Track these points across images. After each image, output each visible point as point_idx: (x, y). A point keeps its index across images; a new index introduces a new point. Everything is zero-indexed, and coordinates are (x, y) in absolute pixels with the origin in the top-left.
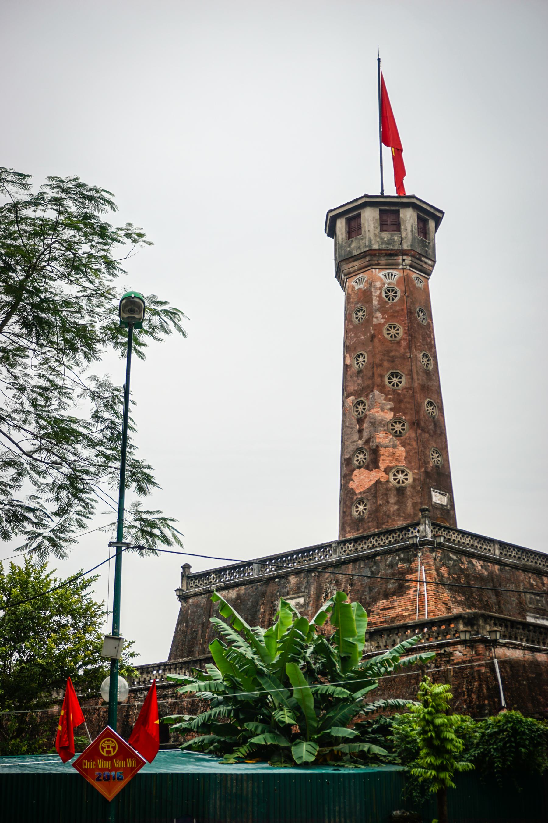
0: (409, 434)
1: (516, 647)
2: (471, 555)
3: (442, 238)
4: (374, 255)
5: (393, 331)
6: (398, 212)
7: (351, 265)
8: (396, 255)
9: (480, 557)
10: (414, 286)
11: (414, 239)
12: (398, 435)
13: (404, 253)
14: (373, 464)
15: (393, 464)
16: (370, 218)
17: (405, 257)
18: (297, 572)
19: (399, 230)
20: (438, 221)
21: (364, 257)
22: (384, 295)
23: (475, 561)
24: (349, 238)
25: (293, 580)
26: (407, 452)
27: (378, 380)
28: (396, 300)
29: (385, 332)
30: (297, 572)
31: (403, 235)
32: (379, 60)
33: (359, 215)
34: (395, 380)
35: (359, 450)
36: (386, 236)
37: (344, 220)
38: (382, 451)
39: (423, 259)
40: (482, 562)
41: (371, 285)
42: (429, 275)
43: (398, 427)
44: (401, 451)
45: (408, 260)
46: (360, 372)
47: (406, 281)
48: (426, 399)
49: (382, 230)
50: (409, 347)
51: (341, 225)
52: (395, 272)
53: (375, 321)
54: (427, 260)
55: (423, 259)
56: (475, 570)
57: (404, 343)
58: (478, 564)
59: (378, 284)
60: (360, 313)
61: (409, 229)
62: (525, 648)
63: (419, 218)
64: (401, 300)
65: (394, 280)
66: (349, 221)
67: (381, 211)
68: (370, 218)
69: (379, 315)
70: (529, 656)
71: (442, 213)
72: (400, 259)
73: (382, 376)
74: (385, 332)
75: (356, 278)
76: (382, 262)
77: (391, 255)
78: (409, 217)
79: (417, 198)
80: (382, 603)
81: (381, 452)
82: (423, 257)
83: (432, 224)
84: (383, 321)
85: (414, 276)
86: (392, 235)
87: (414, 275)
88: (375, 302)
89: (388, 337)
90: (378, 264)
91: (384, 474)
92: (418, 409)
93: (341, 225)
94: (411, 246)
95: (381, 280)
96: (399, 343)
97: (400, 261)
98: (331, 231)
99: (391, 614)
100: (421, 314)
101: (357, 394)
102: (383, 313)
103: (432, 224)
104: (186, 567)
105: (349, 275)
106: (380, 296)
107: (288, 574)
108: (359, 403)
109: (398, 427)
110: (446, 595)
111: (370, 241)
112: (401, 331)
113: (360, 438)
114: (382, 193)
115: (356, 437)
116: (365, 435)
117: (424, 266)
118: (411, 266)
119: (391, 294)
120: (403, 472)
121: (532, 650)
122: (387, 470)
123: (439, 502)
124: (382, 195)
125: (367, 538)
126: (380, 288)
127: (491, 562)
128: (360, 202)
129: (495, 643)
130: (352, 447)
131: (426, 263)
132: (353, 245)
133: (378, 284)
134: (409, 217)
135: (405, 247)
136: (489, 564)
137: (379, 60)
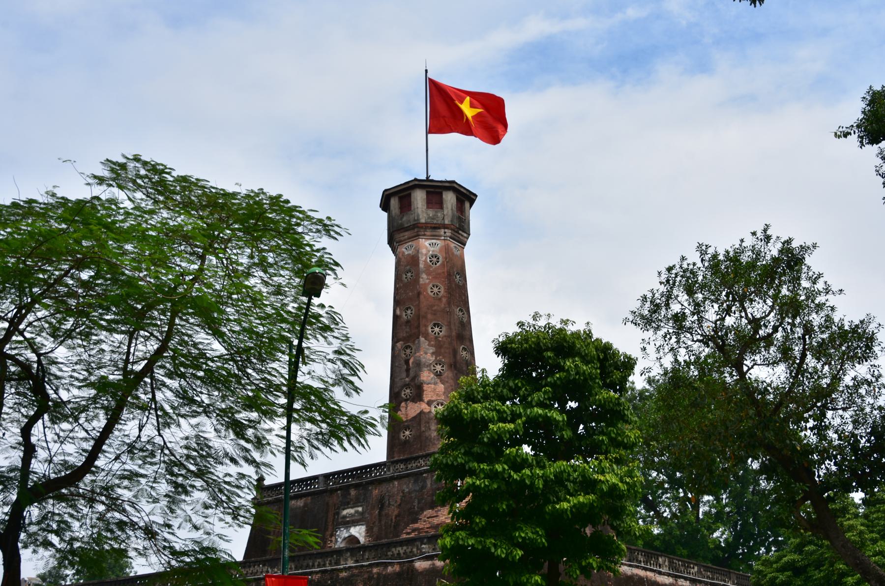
0: (448, 374)
3: (476, 215)
4: (422, 228)
5: (436, 290)
6: (441, 194)
7: (402, 235)
8: (439, 228)
10: (453, 254)
11: (453, 216)
12: (439, 375)
13: (445, 227)
14: (418, 397)
15: (434, 398)
16: (419, 198)
18: (356, 486)
19: (442, 208)
20: (472, 202)
21: (413, 229)
22: (428, 260)
24: (401, 212)
25: (353, 492)
26: (445, 388)
27: (423, 329)
28: (438, 264)
29: (429, 290)
30: (356, 486)
31: (445, 213)
32: (426, 71)
33: (410, 195)
34: (437, 329)
35: (407, 386)
36: (431, 213)
37: (396, 200)
38: (425, 387)
41: (418, 251)
42: (465, 245)
43: (439, 368)
44: (441, 387)
45: (449, 233)
46: (408, 322)
47: (447, 249)
49: (428, 207)
50: (449, 303)
51: (394, 203)
52: (438, 242)
57: (444, 300)
59: (424, 251)
60: (409, 274)
61: (450, 207)
63: (457, 199)
64: (443, 265)
65: (437, 248)
66: (401, 199)
68: (419, 198)
69: (424, 276)
71: (476, 196)
73: (426, 326)
74: (429, 290)
75: (406, 245)
76: (428, 233)
78: (450, 198)
80: (428, 512)
81: (425, 388)
82: (460, 230)
83: (467, 204)
85: (452, 245)
86: (436, 212)
87: (453, 244)
88: (422, 266)
90: (424, 235)
91: (427, 406)
92: (455, 352)
93: (394, 203)
95: (427, 248)
96: (440, 299)
97: (442, 233)
98: (385, 205)
99: (436, 521)
101: (406, 339)
102: (428, 274)
103: (467, 204)
105: (401, 243)
106: (425, 261)
107: (349, 487)
108: (407, 347)
109: (439, 368)
111: (418, 216)
112: (442, 290)
113: (407, 376)
114: (427, 178)
115: (404, 375)
116: (412, 373)
119: (435, 259)
122: (429, 403)
124: (428, 179)
125: (416, 459)
126: (426, 255)
128: (411, 184)
130: (399, 384)
132: (405, 219)
134: (450, 198)
135: (447, 222)
137: (426, 71)
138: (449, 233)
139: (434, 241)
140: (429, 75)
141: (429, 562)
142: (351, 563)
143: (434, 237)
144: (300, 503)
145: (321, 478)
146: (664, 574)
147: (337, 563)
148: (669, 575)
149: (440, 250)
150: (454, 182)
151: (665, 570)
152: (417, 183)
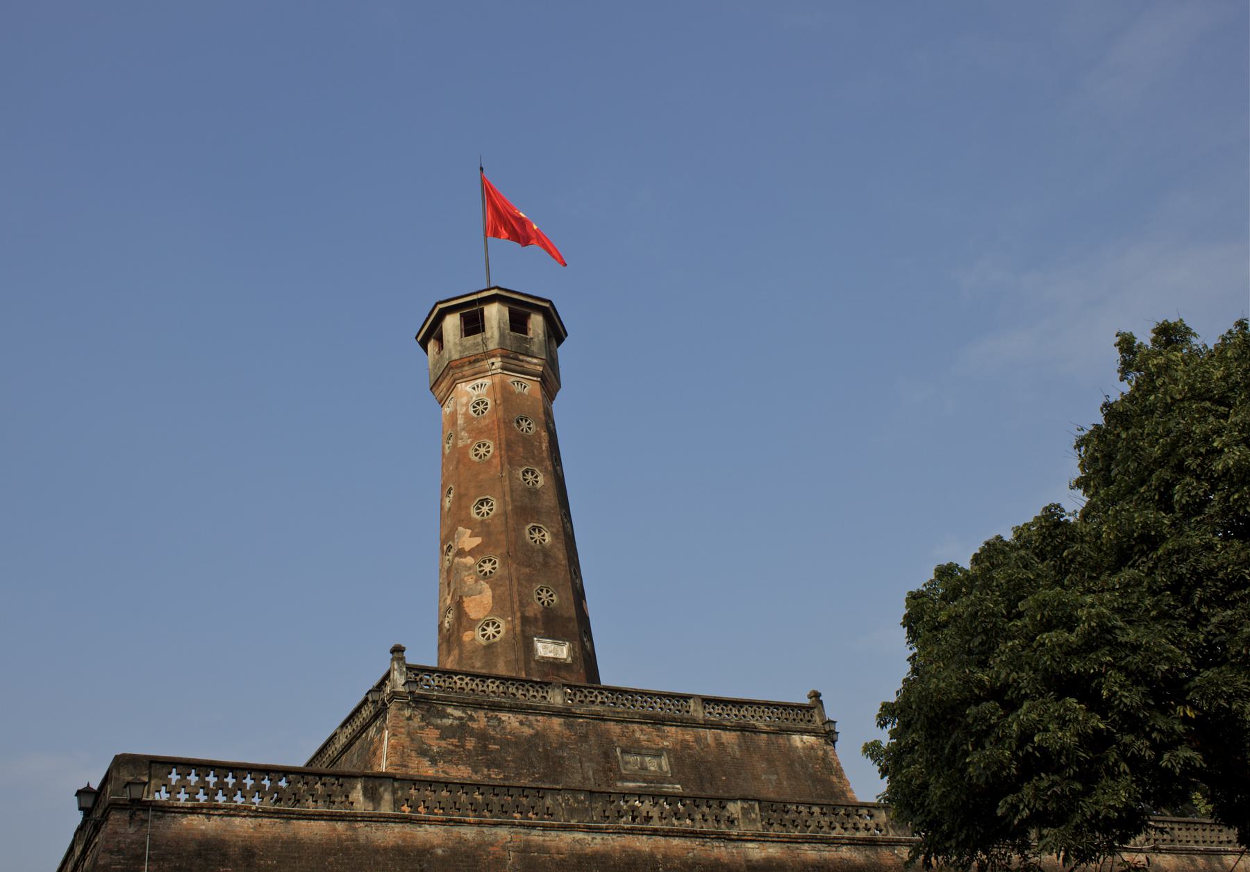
2: (498, 707)
5: (482, 451)
11: (502, 336)
17: (493, 360)
23: (504, 716)
29: (472, 454)
32: (482, 169)
36: (470, 340)
39: (521, 357)
40: (521, 717)
48: (528, 523)
52: (487, 381)
53: (460, 444)
54: (529, 359)
55: (521, 357)
56: (504, 728)
57: (496, 461)
58: (511, 720)
61: (495, 324)
64: (495, 410)
65: (484, 390)
67: (462, 315)
68: (452, 324)
69: (464, 434)
70: (271, 828)
72: (486, 364)
73: (467, 508)
74: (472, 454)
77: (476, 361)
78: (494, 314)
79: (499, 288)
84: (469, 441)
89: (477, 459)
90: (463, 377)
94: (499, 344)
95: (468, 393)
96: (489, 462)
100: (524, 424)
106: (466, 414)
117: (526, 366)
118: (503, 368)
119: (481, 407)
120: (494, 623)
123: (551, 655)
126: (467, 404)
127: (543, 715)
131: (529, 363)
133: (464, 400)
136: (539, 718)
137: (482, 169)
138: (498, 362)
139: (479, 381)
143: (476, 375)
148: (760, 839)
149: (488, 395)
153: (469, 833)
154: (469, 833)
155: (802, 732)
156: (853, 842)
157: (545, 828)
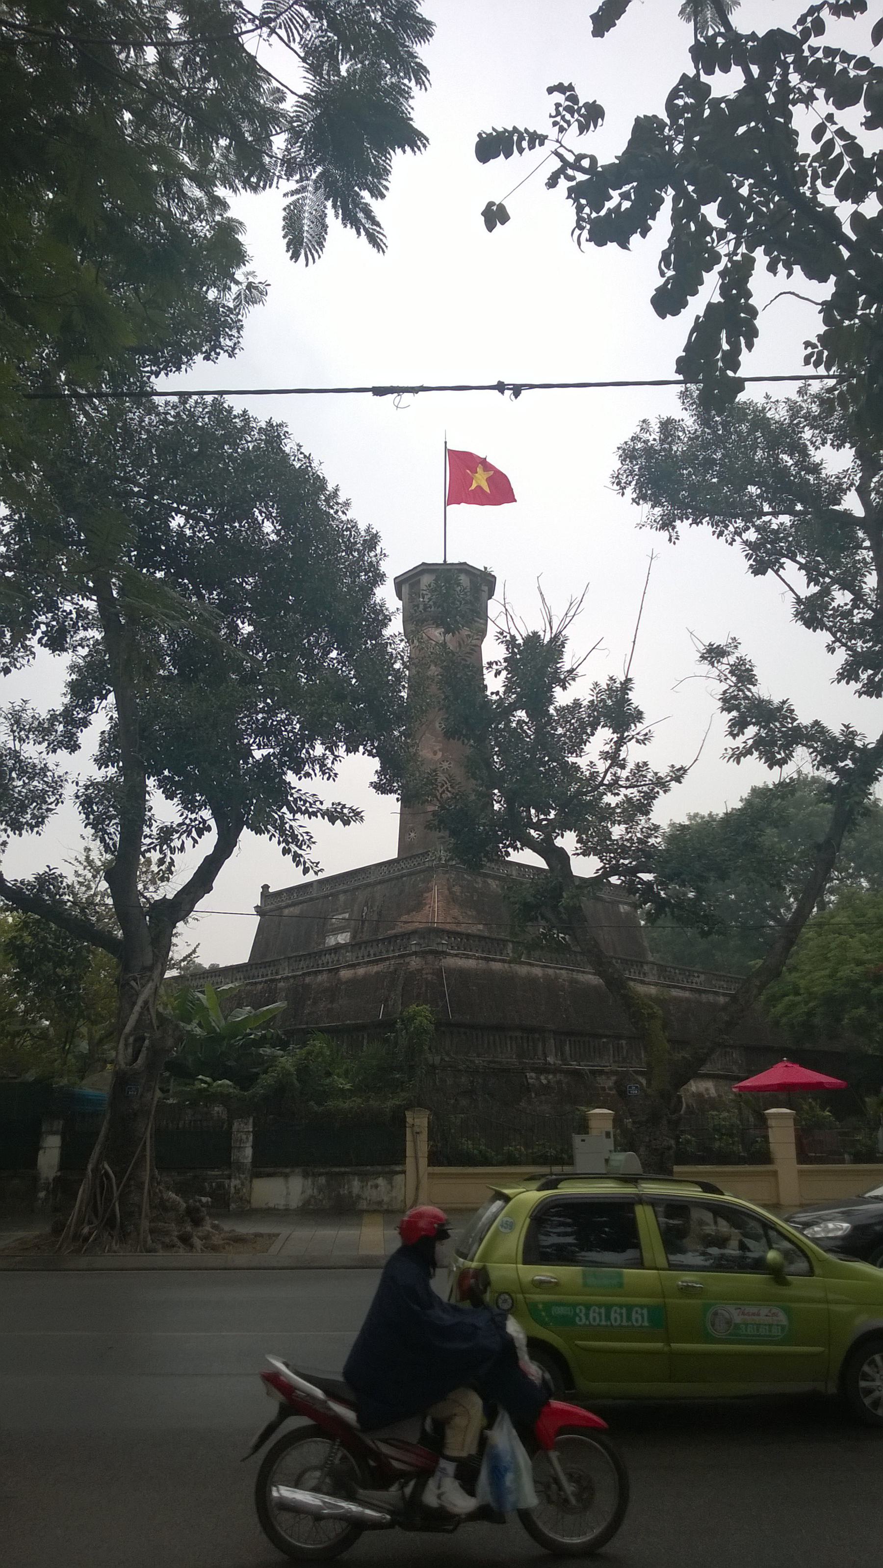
1: (468, 957)
9: (495, 878)
18: (345, 892)
23: (490, 881)
25: (342, 897)
32: (446, 443)
33: (419, 581)
40: (497, 882)
51: (405, 589)
62: (478, 958)
66: (412, 586)
70: (482, 964)
93: (405, 589)
104: (266, 887)
107: (338, 893)
110: (455, 912)
114: (445, 561)
121: (487, 959)
128: (419, 569)
129: (445, 954)
137: (446, 443)
140: (449, 447)
141: (352, 971)
142: (287, 974)
144: (296, 910)
145: (315, 884)
146: (649, 984)
147: (277, 974)
148: (656, 984)
150: (465, 563)
151: (650, 978)
152: (425, 567)
153: (550, 971)
154: (550, 971)
155: (626, 903)
156: (692, 990)
157: (578, 971)
